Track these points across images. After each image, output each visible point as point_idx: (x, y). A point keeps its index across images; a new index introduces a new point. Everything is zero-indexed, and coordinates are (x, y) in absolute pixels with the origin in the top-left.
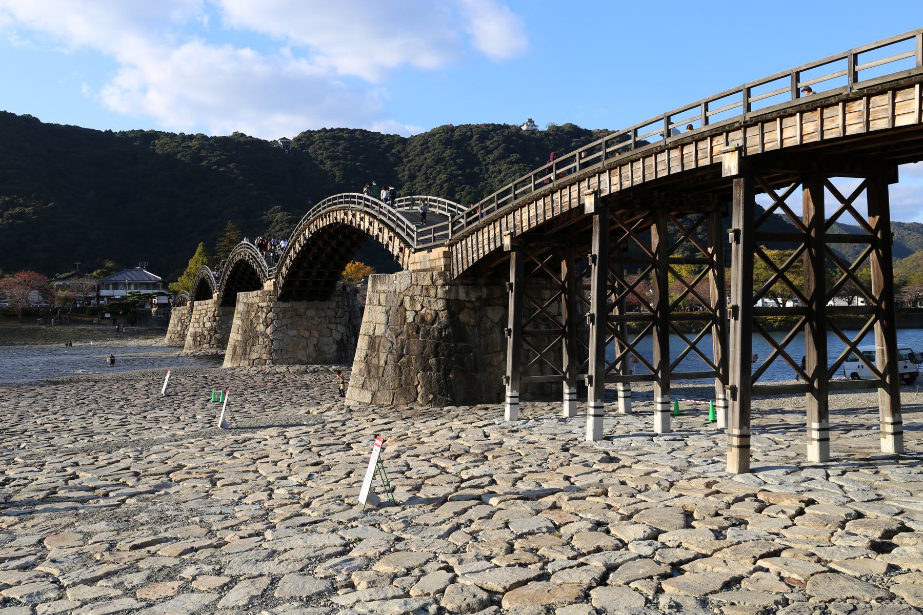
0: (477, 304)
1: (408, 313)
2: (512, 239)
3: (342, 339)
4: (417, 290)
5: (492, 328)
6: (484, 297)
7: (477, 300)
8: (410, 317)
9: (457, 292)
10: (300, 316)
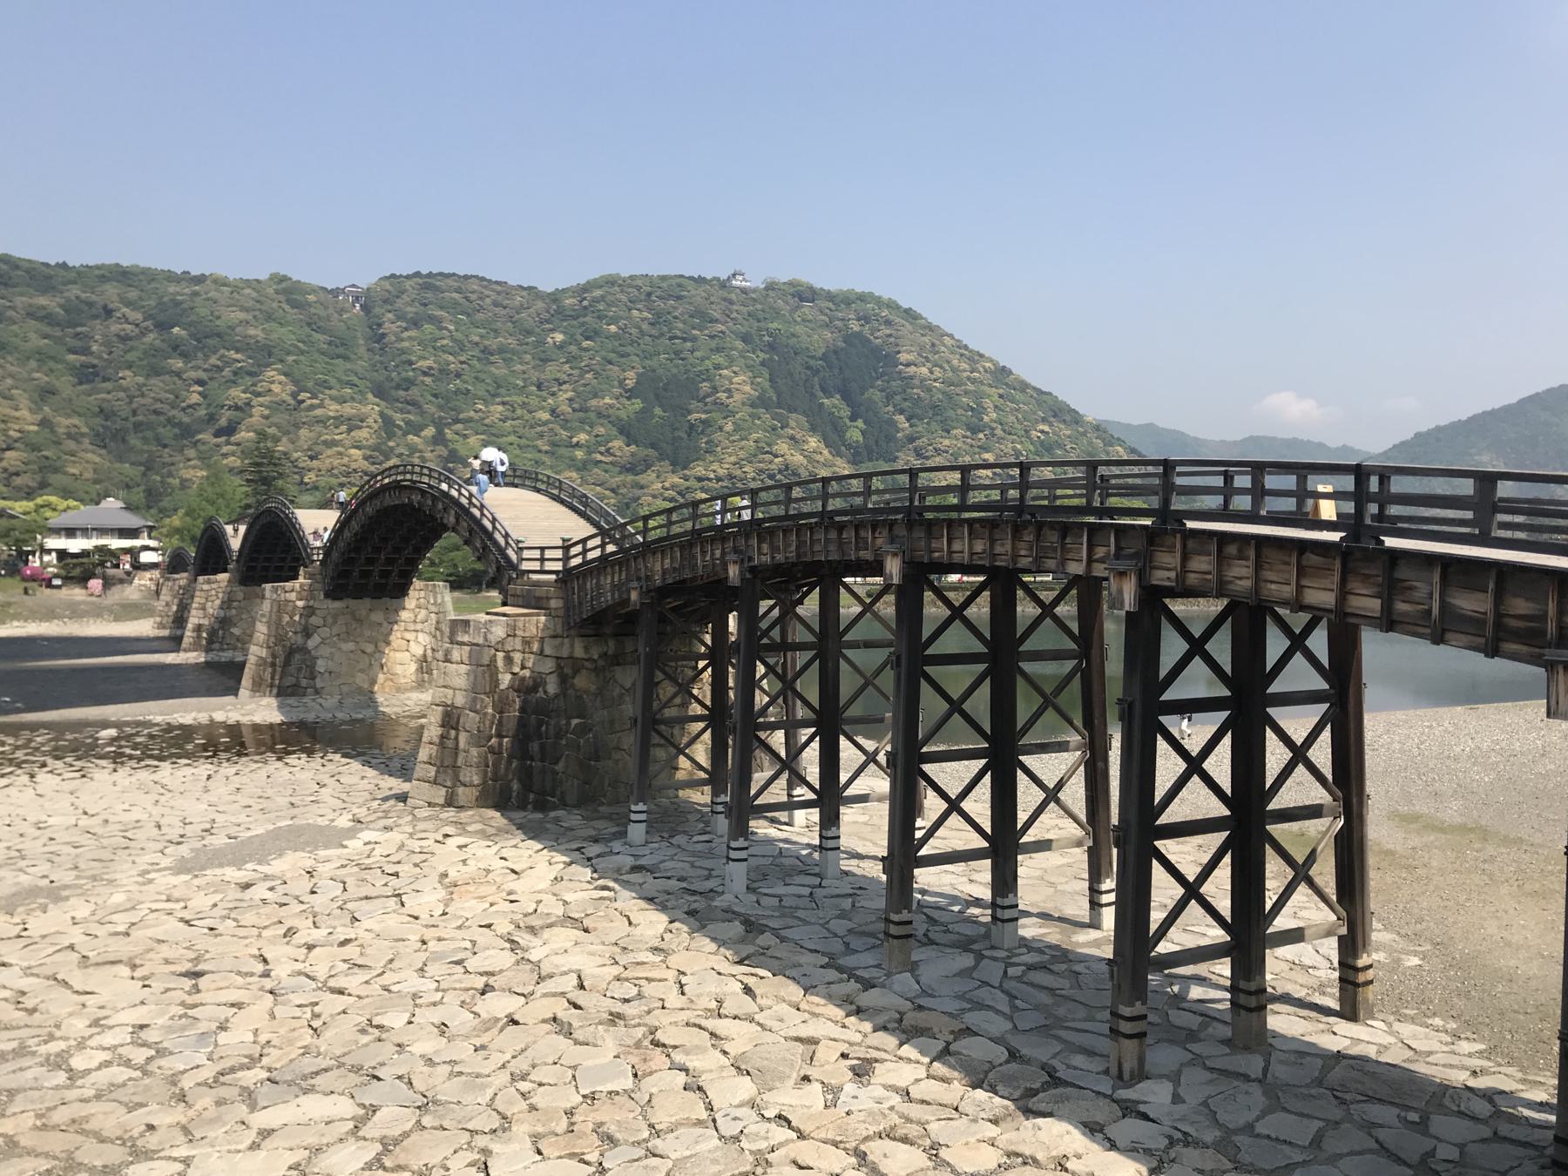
0: (601, 663)
1: (500, 676)
2: (641, 594)
3: (425, 656)
4: (518, 645)
5: (621, 696)
6: (610, 652)
7: (600, 657)
8: (505, 680)
9: (572, 646)
10: (359, 621)
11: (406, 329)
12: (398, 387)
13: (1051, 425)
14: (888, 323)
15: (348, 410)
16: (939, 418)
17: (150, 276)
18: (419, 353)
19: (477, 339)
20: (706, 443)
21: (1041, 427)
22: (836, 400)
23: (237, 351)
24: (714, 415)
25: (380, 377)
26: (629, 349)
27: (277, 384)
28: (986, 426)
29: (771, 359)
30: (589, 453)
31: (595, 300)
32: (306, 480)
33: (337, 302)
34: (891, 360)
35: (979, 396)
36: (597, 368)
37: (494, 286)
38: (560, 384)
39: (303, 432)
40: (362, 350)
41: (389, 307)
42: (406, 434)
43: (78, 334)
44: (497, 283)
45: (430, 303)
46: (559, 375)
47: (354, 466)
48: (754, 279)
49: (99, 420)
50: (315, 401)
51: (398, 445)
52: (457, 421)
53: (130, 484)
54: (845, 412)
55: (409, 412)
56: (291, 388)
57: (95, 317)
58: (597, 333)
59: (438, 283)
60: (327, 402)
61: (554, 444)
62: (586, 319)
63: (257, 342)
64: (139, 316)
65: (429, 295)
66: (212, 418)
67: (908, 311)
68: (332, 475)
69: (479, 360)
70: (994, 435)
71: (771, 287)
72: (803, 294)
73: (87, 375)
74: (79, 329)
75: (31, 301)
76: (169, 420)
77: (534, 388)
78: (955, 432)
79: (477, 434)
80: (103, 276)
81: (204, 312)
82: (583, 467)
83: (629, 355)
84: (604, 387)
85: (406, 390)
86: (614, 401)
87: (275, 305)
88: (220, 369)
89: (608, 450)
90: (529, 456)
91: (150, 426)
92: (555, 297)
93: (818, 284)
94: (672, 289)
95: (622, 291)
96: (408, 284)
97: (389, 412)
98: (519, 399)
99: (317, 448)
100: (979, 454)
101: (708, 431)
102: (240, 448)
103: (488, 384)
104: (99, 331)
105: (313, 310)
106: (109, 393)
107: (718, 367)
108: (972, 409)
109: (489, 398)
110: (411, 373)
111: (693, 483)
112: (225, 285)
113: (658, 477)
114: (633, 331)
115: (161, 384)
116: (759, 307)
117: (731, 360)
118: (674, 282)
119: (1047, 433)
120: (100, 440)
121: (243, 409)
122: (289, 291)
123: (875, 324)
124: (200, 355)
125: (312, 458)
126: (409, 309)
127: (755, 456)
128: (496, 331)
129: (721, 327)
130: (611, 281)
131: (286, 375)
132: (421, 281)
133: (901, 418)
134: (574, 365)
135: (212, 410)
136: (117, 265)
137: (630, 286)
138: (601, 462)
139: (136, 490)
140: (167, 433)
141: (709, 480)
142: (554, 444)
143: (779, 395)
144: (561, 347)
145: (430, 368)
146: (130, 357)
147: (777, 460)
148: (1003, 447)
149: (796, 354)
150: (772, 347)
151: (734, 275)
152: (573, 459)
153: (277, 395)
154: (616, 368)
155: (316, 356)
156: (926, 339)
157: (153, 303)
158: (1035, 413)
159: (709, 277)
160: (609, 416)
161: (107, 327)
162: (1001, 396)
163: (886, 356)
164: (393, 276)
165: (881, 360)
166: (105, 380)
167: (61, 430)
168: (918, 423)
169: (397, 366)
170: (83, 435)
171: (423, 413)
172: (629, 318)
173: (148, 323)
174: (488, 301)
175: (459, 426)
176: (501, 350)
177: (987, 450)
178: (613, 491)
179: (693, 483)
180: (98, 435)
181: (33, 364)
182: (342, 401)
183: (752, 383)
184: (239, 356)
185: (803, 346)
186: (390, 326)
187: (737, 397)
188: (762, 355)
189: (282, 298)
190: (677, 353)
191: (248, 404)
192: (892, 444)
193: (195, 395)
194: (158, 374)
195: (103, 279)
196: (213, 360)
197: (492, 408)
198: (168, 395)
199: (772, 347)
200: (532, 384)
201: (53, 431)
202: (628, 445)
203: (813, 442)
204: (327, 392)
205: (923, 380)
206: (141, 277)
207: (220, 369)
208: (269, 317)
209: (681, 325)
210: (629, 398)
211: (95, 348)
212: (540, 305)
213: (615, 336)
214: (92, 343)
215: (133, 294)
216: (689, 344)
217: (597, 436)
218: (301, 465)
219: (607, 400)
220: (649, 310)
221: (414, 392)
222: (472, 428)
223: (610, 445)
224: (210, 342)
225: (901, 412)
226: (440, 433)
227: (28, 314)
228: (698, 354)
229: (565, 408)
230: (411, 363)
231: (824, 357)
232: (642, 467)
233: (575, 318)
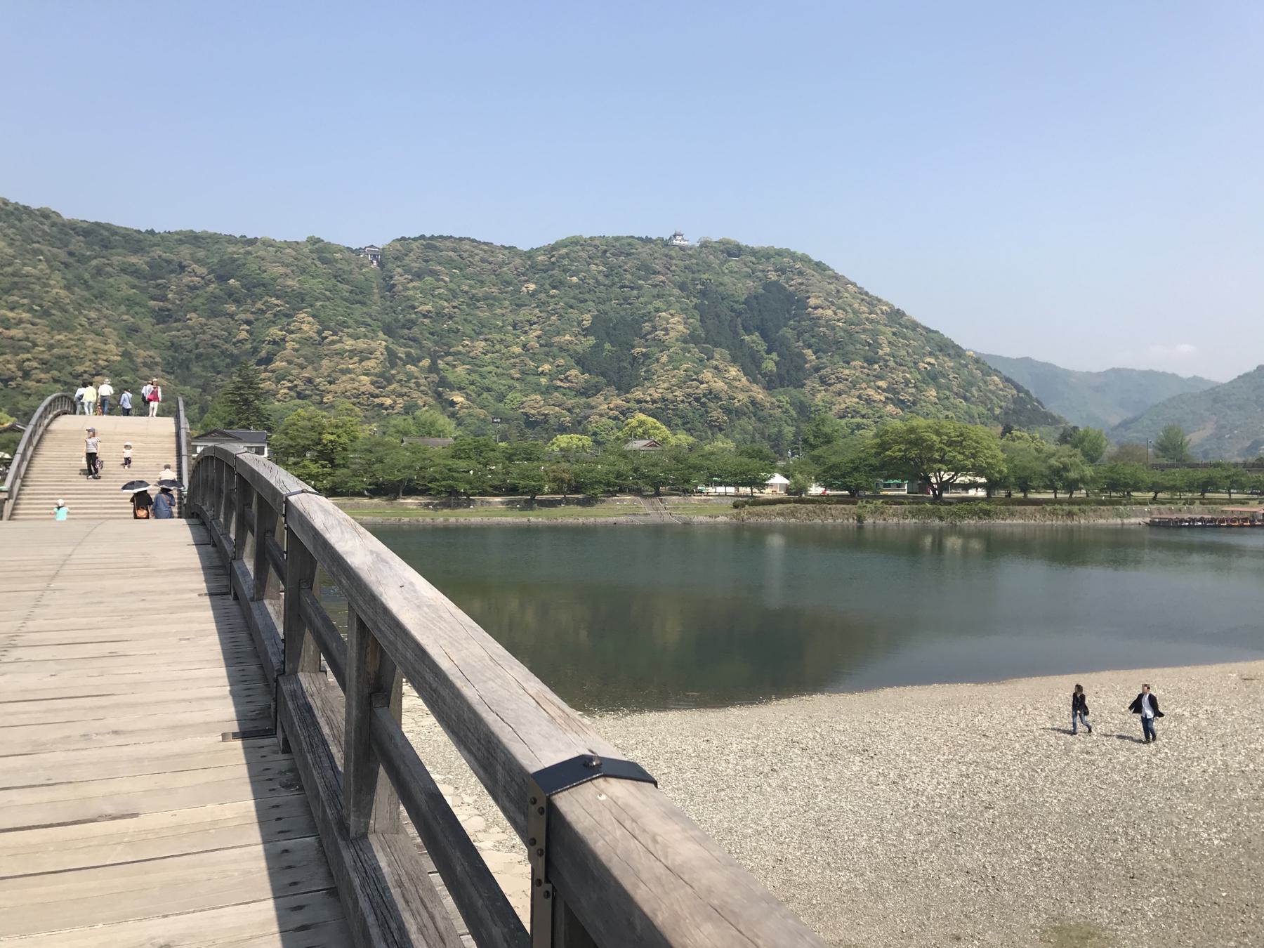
11: (412, 281)
12: (403, 327)
13: (937, 358)
14: (801, 273)
15: (361, 344)
16: (841, 351)
17: (216, 238)
18: (421, 300)
19: (466, 288)
20: (645, 372)
21: (928, 360)
22: (756, 337)
23: (278, 297)
24: (652, 349)
25: (388, 319)
26: (587, 296)
27: (306, 324)
28: (881, 358)
29: (702, 304)
32: (325, 400)
33: (358, 259)
34: (802, 304)
35: (875, 333)
37: (482, 246)
38: (531, 325)
39: (325, 362)
40: (376, 297)
41: (399, 263)
42: (405, 364)
43: (158, 285)
45: (431, 260)
46: (530, 317)
47: (363, 389)
48: (691, 240)
49: (171, 353)
50: (335, 337)
51: (398, 373)
52: (448, 354)
53: (190, 402)
54: (762, 347)
55: (411, 347)
56: (317, 327)
57: (172, 271)
58: (561, 282)
59: (438, 244)
60: (344, 338)
61: (524, 373)
62: (553, 272)
63: (293, 290)
64: (203, 271)
65: (431, 253)
66: (255, 351)
67: (818, 264)
68: (345, 397)
69: (468, 305)
70: (887, 366)
71: (705, 245)
72: (732, 250)
73: (163, 317)
74: (160, 281)
75: (125, 260)
76: (222, 352)
77: (510, 328)
78: (853, 363)
79: (464, 364)
80: (180, 240)
81: (254, 267)
82: (546, 391)
84: (565, 326)
85: (409, 329)
86: (573, 338)
87: (309, 261)
88: (264, 312)
90: (503, 382)
91: (209, 357)
92: (530, 255)
93: (744, 242)
94: (623, 247)
95: (583, 250)
96: (414, 245)
97: (394, 347)
98: (498, 337)
99: (334, 375)
100: (874, 381)
101: (647, 362)
102: (275, 375)
103: (475, 325)
104: (174, 284)
105: (339, 266)
106: (179, 331)
107: (658, 310)
108: (869, 344)
109: (474, 335)
110: (414, 316)
111: (633, 405)
112: (271, 246)
113: (605, 399)
114: (591, 281)
115: (218, 324)
116: (694, 261)
117: (669, 305)
118: (625, 242)
119: (933, 365)
120: (169, 369)
121: (278, 343)
122: (320, 250)
123: (790, 274)
124: (249, 301)
125: (330, 383)
126: (414, 264)
127: (685, 382)
128: (482, 282)
129: (661, 278)
130: (574, 242)
131: (314, 316)
132: (425, 243)
133: (808, 352)
134: (542, 308)
135: (255, 344)
136: (192, 231)
137: (590, 245)
138: (561, 387)
139: (192, 407)
140: (221, 363)
141: (646, 402)
142: (524, 373)
143: (707, 332)
144: (533, 295)
145: (429, 312)
146: (196, 303)
148: (894, 376)
149: (723, 299)
150: (703, 294)
151: (675, 236)
152: (538, 385)
153: (306, 332)
154: (576, 311)
155: (339, 301)
156: (832, 287)
157: (216, 261)
158: (923, 348)
159: (654, 238)
160: (568, 351)
161: (180, 279)
162: (894, 334)
163: (798, 301)
164: (403, 238)
165: (793, 304)
166: (177, 320)
167: (139, 360)
168: (824, 356)
169: (402, 310)
170: (156, 364)
171: (421, 347)
174: (477, 258)
175: (450, 358)
176: (486, 298)
177: (881, 378)
178: (569, 410)
179: (633, 405)
180: (168, 363)
181: (123, 308)
182: (356, 337)
183: (685, 323)
184: (278, 302)
185: (730, 293)
186: (399, 279)
187: (672, 334)
188: (695, 300)
189: (314, 256)
190: (625, 299)
191: (283, 340)
192: (801, 373)
195: (181, 242)
196: (259, 305)
197: (477, 344)
198: (223, 333)
199: (703, 294)
200: (509, 324)
201: (132, 361)
202: (582, 374)
203: (733, 371)
204: (346, 330)
206: (209, 240)
207: (264, 312)
208: (303, 271)
209: (629, 276)
210: (585, 336)
212: (518, 261)
213: (577, 286)
214: (169, 292)
215: (201, 254)
216: (635, 292)
217: (558, 366)
218: (323, 388)
219: (568, 337)
221: (415, 330)
222: (459, 360)
223: (568, 373)
224: (257, 291)
225: (809, 346)
226: (434, 363)
227: (122, 270)
228: (642, 300)
229: (534, 344)
230: (413, 307)
231: (746, 302)
232: (593, 392)
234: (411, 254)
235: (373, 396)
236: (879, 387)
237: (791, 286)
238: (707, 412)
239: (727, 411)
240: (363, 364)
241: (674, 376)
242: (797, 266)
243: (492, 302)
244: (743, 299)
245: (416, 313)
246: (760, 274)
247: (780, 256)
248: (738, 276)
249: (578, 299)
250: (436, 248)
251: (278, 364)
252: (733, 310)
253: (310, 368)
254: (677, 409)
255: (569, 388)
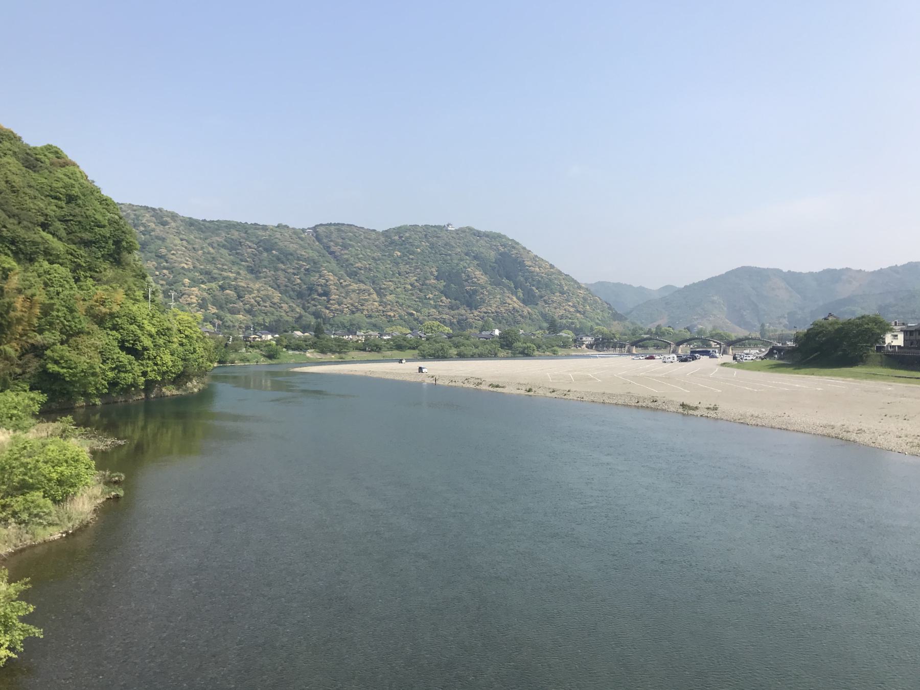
11: (342, 250)
14: (514, 247)
19: (370, 254)
21: (579, 291)
26: (429, 260)
30: (434, 302)
31: (407, 238)
34: (522, 263)
36: (420, 267)
38: (407, 273)
44: (361, 228)
46: (406, 270)
54: (513, 286)
56: (337, 278)
70: (569, 295)
71: (462, 230)
72: (478, 234)
74: (238, 251)
76: (292, 289)
78: (556, 294)
79: (391, 294)
82: (435, 307)
83: (428, 262)
85: (356, 276)
88: (299, 269)
89: (441, 301)
92: (386, 233)
93: (479, 230)
96: (332, 228)
107: (465, 267)
108: (560, 285)
110: (355, 269)
111: (482, 314)
113: (466, 311)
118: (433, 229)
124: (288, 263)
144: (400, 257)
146: (266, 263)
147: (510, 306)
151: (448, 225)
154: (428, 267)
160: (435, 287)
163: (519, 263)
166: (260, 273)
168: (541, 290)
172: (423, 246)
173: (260, 248)
177: (568, 300)
178: (452, 317)
183: (482, 275)
184: (304, 264)
186: (333, 249)
190: (445, 261)
193: (298, 280)
194: (278, 271)
199: (475, 258)
203: (515, 299)
205: (537, 273)
207: (299, 269)
211: (248, 259)
216: (449, 257)
217: (435, 295)
218: (360, 308)
220: (428, 242)
223: (442, 299)
229: (416, 284)
230: (352, 265)
231: (496, 262)
233: (401, 245)
234: (333, 234)
235: (383, 312)
236: (569, 305)
237: (513, 254)
238: (515, 317)
239: (522, 316)
240: (371, 296)
241: (496, 301)
242: (510, 244)
243: (383, 261)
244: (494, 260)
245: (355, 267)
246: (495, 248)
247: (500, 237)
248: (485, 248)
249: (425, 261)
250: (342, 231)
251: (333, 297)
252: (490, 266)
253: (348, 298)
254: (503, 316)
255: (445, 306)
